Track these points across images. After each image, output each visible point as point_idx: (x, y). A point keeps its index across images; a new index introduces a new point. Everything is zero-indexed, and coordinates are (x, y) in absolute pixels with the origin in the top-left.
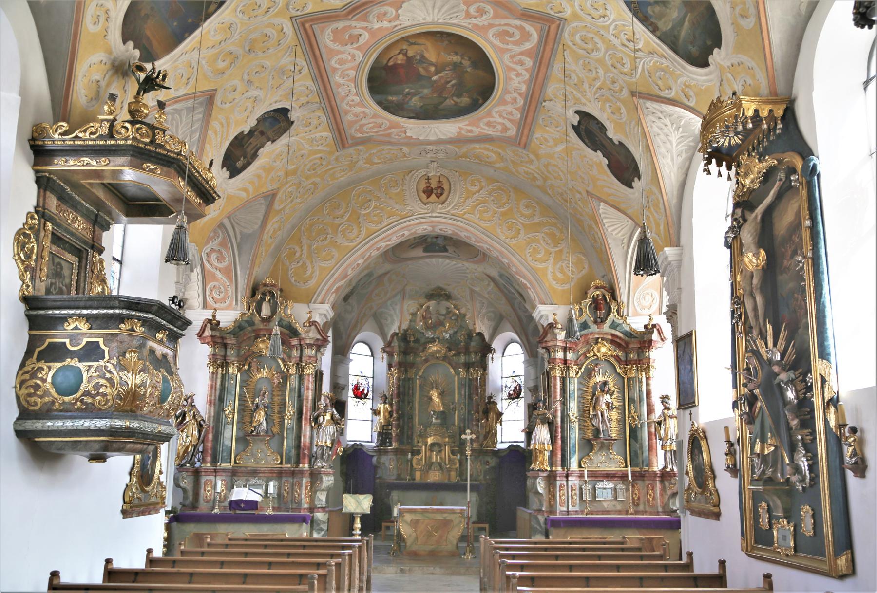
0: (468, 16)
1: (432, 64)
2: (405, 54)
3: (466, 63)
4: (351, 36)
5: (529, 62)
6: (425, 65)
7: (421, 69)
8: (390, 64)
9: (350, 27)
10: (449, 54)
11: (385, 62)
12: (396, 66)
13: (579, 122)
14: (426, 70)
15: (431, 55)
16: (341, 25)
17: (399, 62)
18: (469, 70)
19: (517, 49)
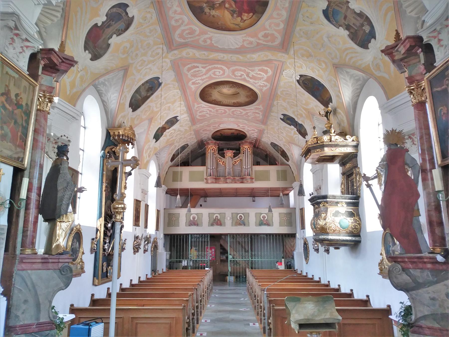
0: (211, 39)
1: (227, 8)
2: (242, 19)
3: (207, 10)
4: (267, 37)
5: (173, 23)
6: (231, 9)
7: (234, 6)
8: (251, 14)
9: (266, 41)
10: (217, 16)
11: (254, 16)
12: (248, 13)
13: (127, 14)
14: (231, 6)
15: (227, 15)
16: (270, 44)
17: (246, 14)
18: (205, 5)
19: (182, 28)
